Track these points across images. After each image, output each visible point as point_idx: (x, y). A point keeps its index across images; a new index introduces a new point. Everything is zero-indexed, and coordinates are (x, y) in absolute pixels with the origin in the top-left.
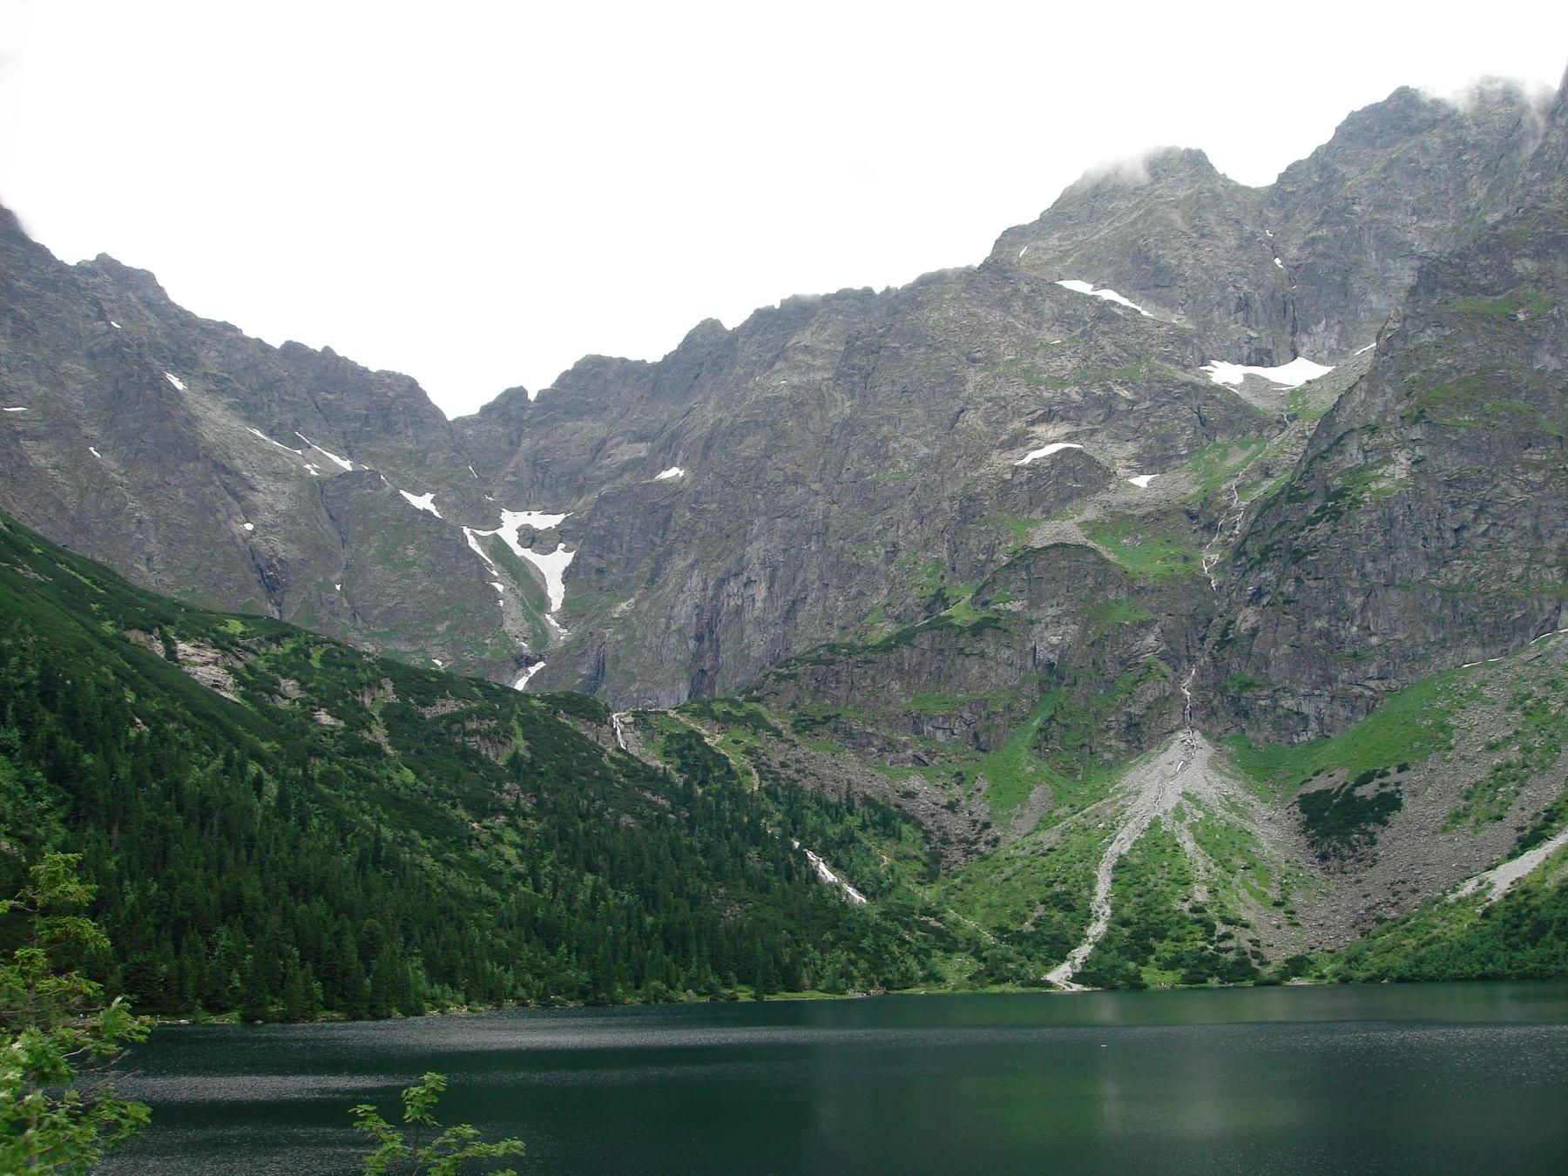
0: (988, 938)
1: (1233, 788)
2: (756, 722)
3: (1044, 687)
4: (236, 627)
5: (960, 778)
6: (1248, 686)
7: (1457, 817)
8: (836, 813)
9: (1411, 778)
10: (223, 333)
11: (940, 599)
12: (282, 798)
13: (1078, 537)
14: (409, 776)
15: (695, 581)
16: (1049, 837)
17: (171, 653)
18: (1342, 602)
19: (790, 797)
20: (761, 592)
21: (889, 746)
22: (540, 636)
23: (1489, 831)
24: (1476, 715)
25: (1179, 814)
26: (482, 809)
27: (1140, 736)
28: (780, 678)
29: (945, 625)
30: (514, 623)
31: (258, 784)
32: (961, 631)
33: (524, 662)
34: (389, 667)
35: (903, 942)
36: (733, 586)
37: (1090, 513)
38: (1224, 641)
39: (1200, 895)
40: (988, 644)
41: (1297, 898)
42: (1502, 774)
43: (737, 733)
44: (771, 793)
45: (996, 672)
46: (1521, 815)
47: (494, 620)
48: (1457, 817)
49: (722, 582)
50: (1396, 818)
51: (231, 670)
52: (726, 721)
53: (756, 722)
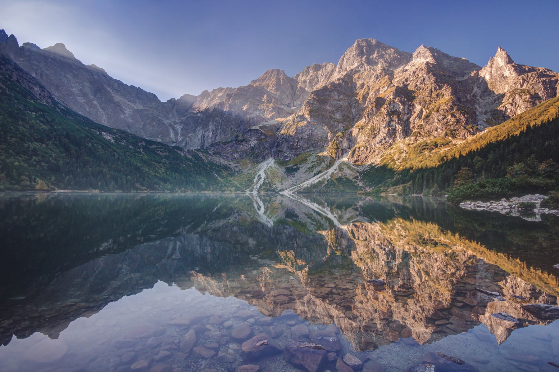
0: (238, 185)
1: (276, 165)
2: (207, 153)
3: (251, 150)
4: (115, 131)
5: (238, 162)
6: (280, 151)
7: (306, 171)
8: (218, 166)
9: (301, 166)
10: (119, 83)
11: (238, 136)
12: (118, 158)
13: (258, 128)
14: (146, 157)
15: (201, 131)
16: (250, 172)
17: (100, 134)
18: (295, 140)
19: (211, 164)
20: (211, 134)
21: (227, 157)
22: (177, 139)
23: (311, 173)
24: (311, 158)
25: (268, 169)
26: (158, 162)
27: (264, 158)
28: (211, 146)
29: (238, 140)
30: (172, 135)
31: (114, 156)
32: (240, 141)
33: (174, 143)
34: (144, 140)
35: (225, 185)
36: (207, 133)
37: (261, 125)
38: (278, 145)
39: (269, 180)
40: (243, 143)
41: (283, 182)
42: (313, 166)
43: (204, 154)
44: (208, 163)
45: (245, 147)
46: (315, 171)
47: (168, 135)
48: (306, 171)
49: (205, 132)
50: (298, 171)
51: (113, 137)
52: (202, 152)
53: (207, 153)
